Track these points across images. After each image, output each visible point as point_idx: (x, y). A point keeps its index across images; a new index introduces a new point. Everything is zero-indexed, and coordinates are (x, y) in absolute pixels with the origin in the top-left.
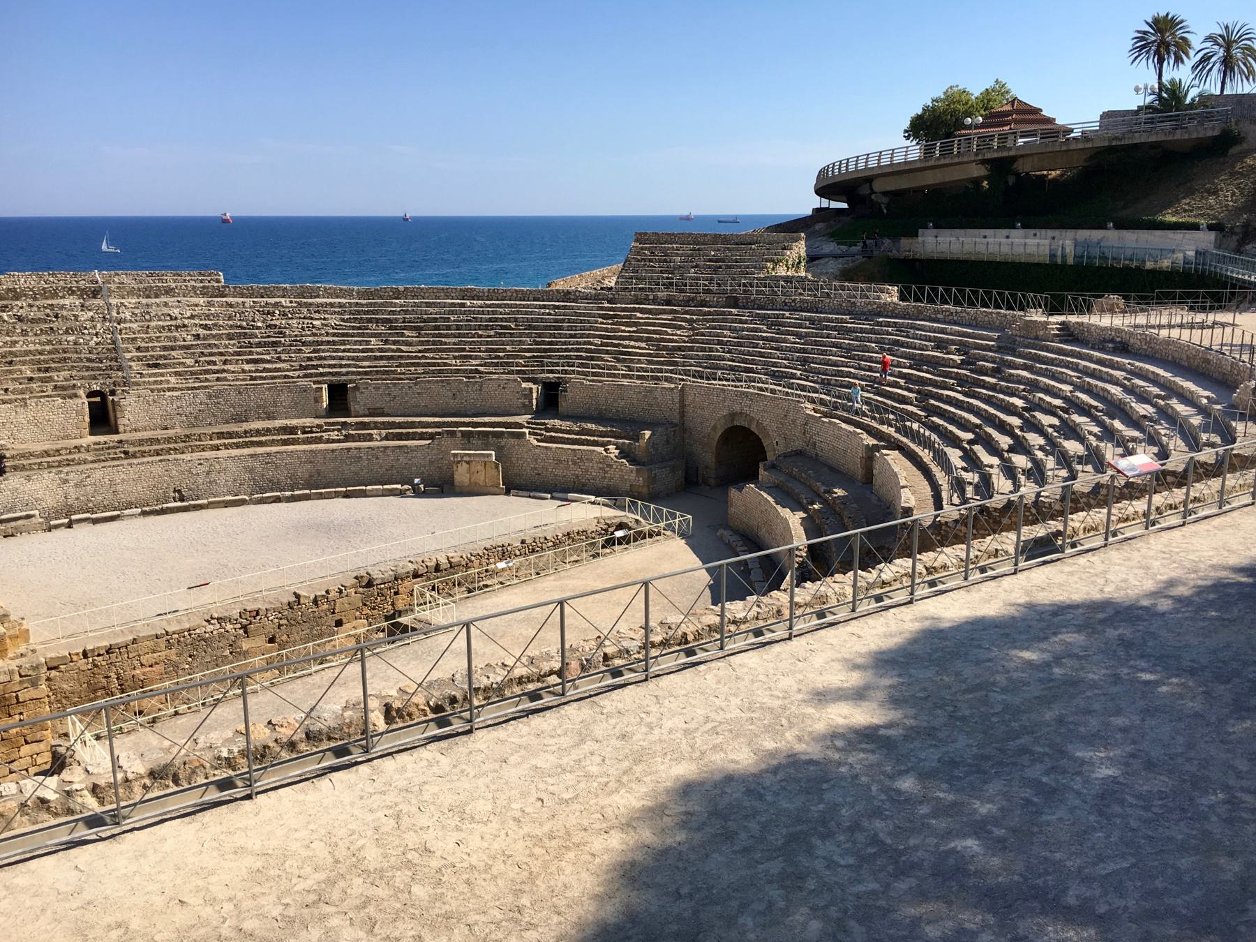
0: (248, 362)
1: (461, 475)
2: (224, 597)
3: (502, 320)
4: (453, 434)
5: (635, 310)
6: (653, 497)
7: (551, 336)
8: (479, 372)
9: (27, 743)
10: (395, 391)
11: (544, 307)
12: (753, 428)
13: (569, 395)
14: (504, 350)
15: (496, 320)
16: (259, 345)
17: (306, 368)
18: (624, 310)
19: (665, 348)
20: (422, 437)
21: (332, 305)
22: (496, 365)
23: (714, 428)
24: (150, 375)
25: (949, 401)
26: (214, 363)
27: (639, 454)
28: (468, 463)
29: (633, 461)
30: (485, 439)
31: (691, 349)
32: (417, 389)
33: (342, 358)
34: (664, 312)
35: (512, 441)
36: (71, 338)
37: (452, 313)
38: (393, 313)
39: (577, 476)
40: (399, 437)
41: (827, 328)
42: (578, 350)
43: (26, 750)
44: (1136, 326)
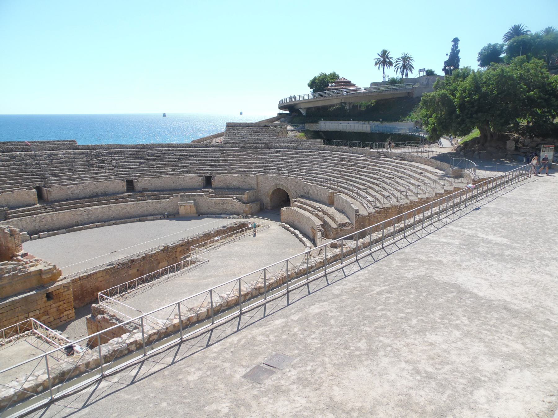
0: (94, 173)
1: (182, 210)
2: (122, 256)
4: (177, 196)
5: (232, 150)
9: (66, 311)
10: (152, 182)
11: (199, 150)
16: (96, 167)
17: (116, 175)
18: (228, 150)
19: (247, 163)
21: (121, 152)
23: (270, 190)
25: (352, 177)
27: (245, 200)
30: (189, 198)
31: (256, 163)
34: (243, 151)
35: (199, 197)
36: (23, 166)
41: (302, 154)
42: (215, 165)
43: (65, 313)
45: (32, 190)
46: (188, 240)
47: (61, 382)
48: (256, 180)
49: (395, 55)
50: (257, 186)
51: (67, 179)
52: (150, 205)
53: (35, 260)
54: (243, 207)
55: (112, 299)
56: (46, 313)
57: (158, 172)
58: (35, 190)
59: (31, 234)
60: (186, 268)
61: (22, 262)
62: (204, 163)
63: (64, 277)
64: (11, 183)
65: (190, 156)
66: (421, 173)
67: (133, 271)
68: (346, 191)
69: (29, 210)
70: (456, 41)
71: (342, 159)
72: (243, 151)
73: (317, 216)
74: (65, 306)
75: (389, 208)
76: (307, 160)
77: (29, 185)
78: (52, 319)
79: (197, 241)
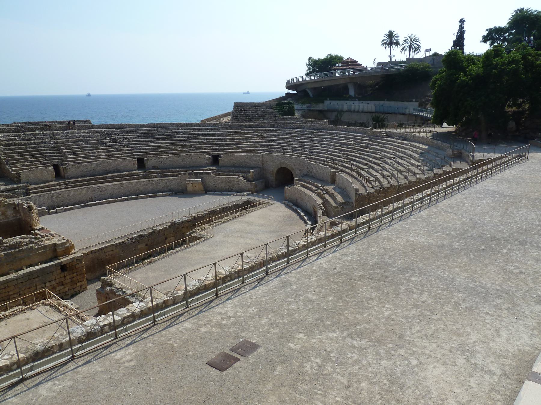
1: (190, 188)
3: (193, 134)
4: (185, 174)
5: (239, 129)
7: (212, 139)
9: (79, 282)
10: (162, 160)
11: (207, 129)
13: (223, 159)
14: (196, 145)
15: (191, 134)
16: (109, 146)
18: (235, 129)
19: (253, 142)
20: (173, 176)
21: (133, 131)
22: (195, 150)
25: (355, 156)
26: (95, 153)
29: (248, 180)
30: (197, 176)
31: (262, 142)
33: (140, 149)
34: (250, 130)
35: (206, 175)
37: (175, 132)
38: (154, 133)
40: (165, 176)
41: (307, 134)
43: (78, 284)
44: (408, 132)
45: (50, 168)
47: (34, 360)
50: (263, 164)
51: (83, 157)
52: (158, 181)
53: (51, 234)
54: (248, 185)
55: (119, 273)
56: (61, 284)
57: (167, 151)
58: (52, 167)
59: (49, 209)
60: (191, 244)
61: (39, 236)
62: (212, 142)
63: (77, 250)
64: (31, 161)
65: (199, 135)
68: (347, 170)
69: (47, 187)
70: (462, 21)
72: (250, 130)
73: (318, 195)
74: (78, 277)
75: (388, 188)
76: (311, 140)
77: (48, 163)
78: (66, 289)
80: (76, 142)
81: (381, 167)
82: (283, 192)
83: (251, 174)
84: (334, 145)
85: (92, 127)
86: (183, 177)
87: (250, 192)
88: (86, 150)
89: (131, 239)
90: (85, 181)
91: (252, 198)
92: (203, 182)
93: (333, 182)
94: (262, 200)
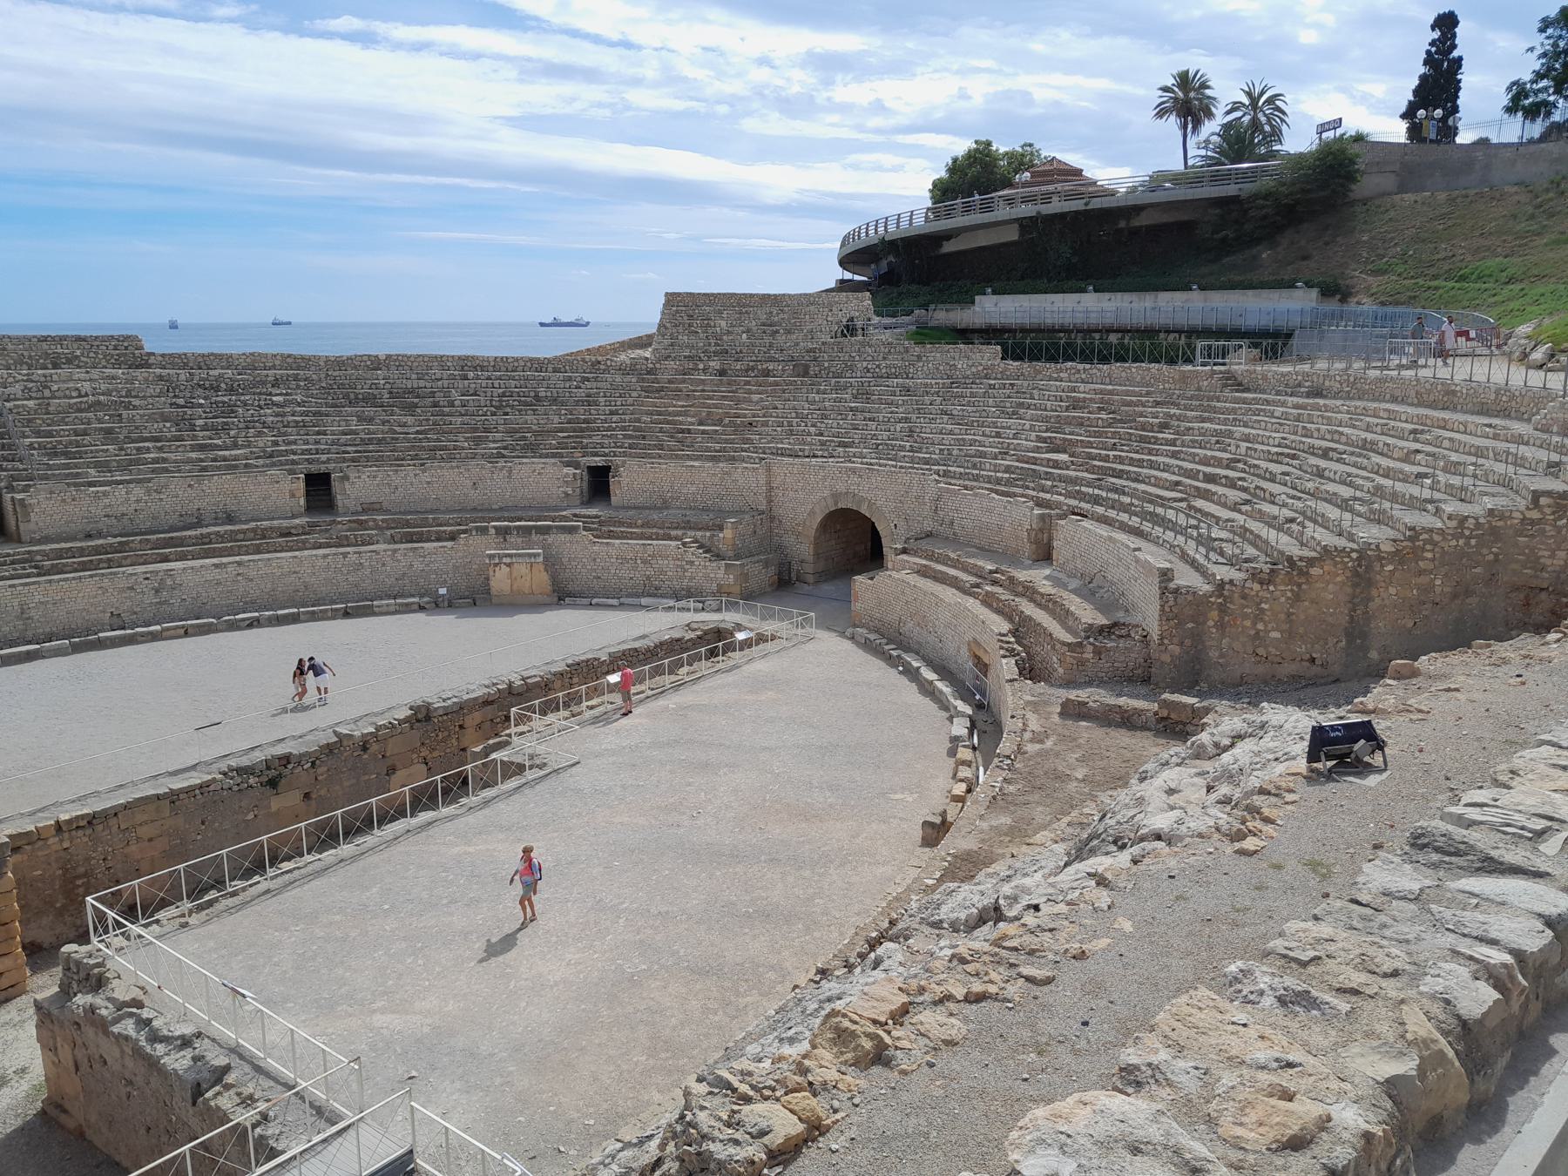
0: (193, 448)
1: (500, 580)
6: (749, 596)
8: (504, 456)
11: (570, 379)
12: (864, 510)
13: (625, 480)
23: (812, 513)
24: (59, 467)
25: (1121, 460)
26: (148, 450)
28: (509, 565)
32: (426, 477)
35: (563, 537)
39: (648, 578)
40: (410, 538)
46: (510, 684)
48: (762, 480)
49: (1226, 91)
50: (770, 501)
51: (97, 465)
52: (385, 559)
54: (718, 573)
60: (488, 793)
66: (1414, 432)
67: (289, 799)
68: (1100, 510)
71: (1076, 405)
73: (988, 601)
75: (1311, 562)
79: (545, 686)
80: (80, 411)
81: (1245, 490)
82: (847, 599)
83: (728, 533)
84: (1032, 429)
85: (143, 362)
86: (476, 541)
87: (724, 597)
88: (114, 441)
89: (240, 771)
90: (97, 551)
91: (728, 618)
92: (551, 563)
93: (1045, 555)
94: (769, 627)
